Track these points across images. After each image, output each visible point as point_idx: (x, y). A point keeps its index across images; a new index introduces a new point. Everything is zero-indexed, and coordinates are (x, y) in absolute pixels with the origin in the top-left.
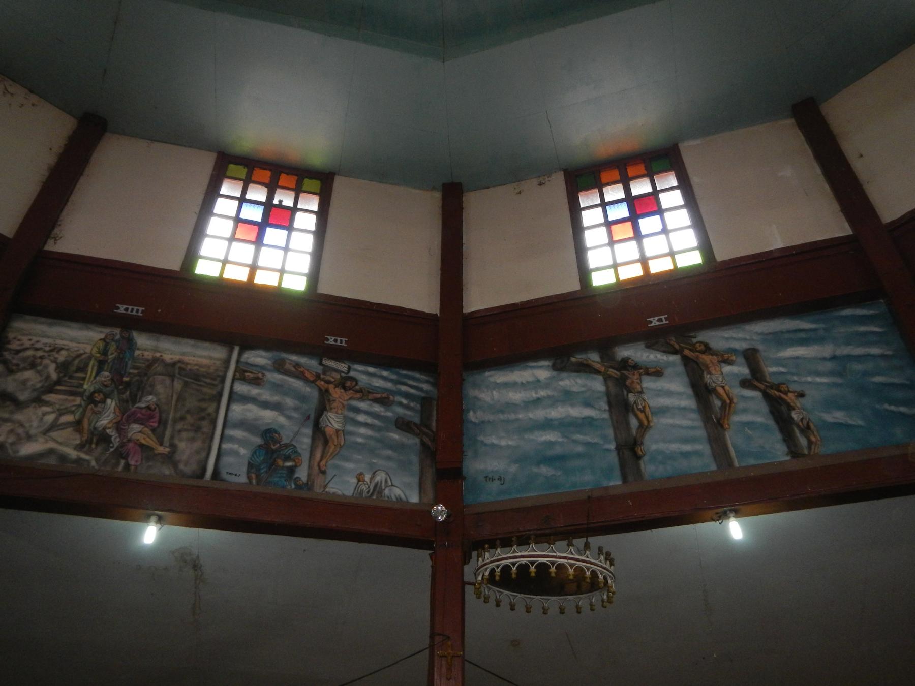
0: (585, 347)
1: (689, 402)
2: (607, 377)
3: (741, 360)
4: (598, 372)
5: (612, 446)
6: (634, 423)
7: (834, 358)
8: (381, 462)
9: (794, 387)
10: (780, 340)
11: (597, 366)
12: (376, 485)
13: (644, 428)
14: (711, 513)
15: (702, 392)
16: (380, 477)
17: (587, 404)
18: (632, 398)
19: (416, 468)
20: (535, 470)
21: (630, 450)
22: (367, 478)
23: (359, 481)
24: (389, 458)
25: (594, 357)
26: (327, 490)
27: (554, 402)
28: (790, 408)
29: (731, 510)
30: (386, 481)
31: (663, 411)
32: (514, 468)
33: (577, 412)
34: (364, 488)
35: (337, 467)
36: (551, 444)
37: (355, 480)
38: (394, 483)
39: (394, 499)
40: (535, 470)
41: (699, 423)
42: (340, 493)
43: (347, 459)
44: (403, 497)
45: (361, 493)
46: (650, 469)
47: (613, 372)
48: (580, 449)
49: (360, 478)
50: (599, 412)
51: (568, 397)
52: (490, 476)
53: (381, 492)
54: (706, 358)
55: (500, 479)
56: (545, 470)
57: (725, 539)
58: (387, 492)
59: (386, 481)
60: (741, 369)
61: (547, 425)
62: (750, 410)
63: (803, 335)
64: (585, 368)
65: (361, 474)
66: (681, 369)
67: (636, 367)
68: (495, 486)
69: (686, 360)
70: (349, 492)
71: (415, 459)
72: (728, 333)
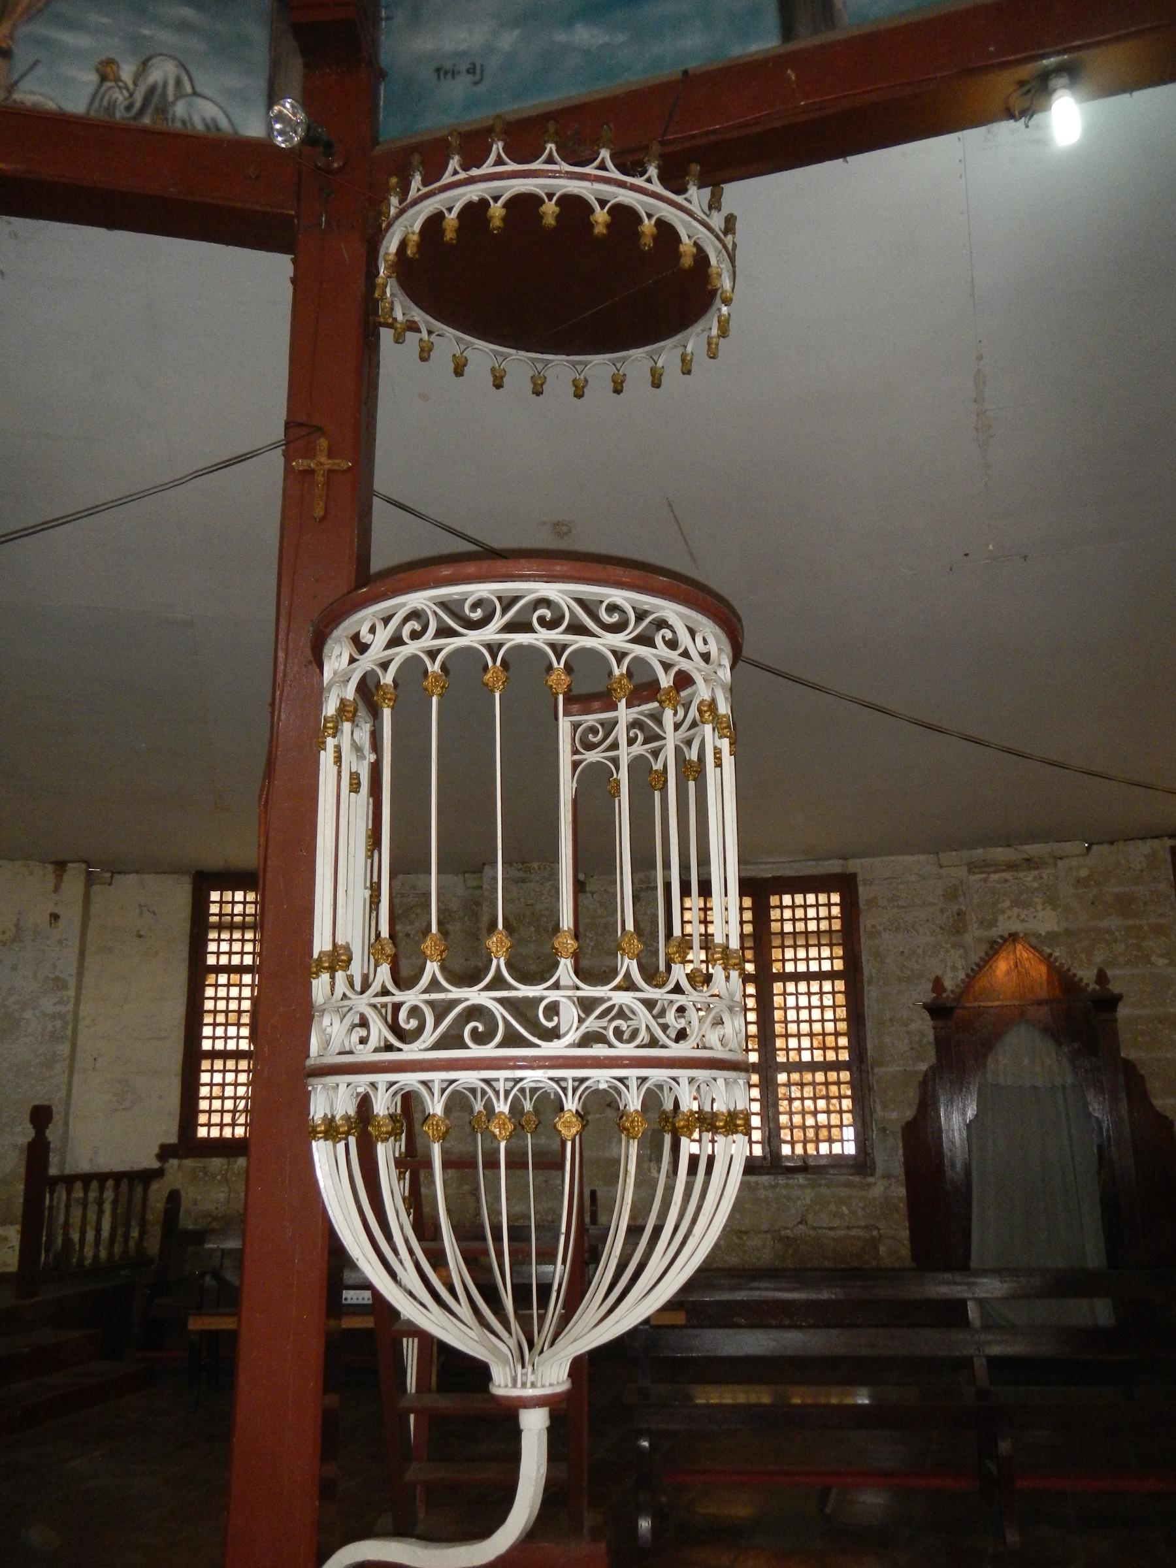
8: (166, 37)
12: (152, 90)
14: (1004, 81)
16: (162, 72)
19: (260, 56)
20: (561, 37)
22: (127, 72)
23: (104, 78)
24: (185, 27)
26: (17, 96)
29: (1060, 69)
30: (178, 82)
32: (508, 40)
34: (120, 97)
35: (41, 42)
37: (93, 78)
38: (199, 89)
39: (200, 126)
40: (561, 37)
42: (51, 105)
43: (71, 25)
44: (224, 123)
45: (112, 105)
49: (106, 72)
52: (448, 65)
53: (163, 110)
55: (471, 71)
58: (180, 109)
59: (178, 82)
65: (110, 62)
68: (458, 89)
70: (76, 104)
71: (258, 34)
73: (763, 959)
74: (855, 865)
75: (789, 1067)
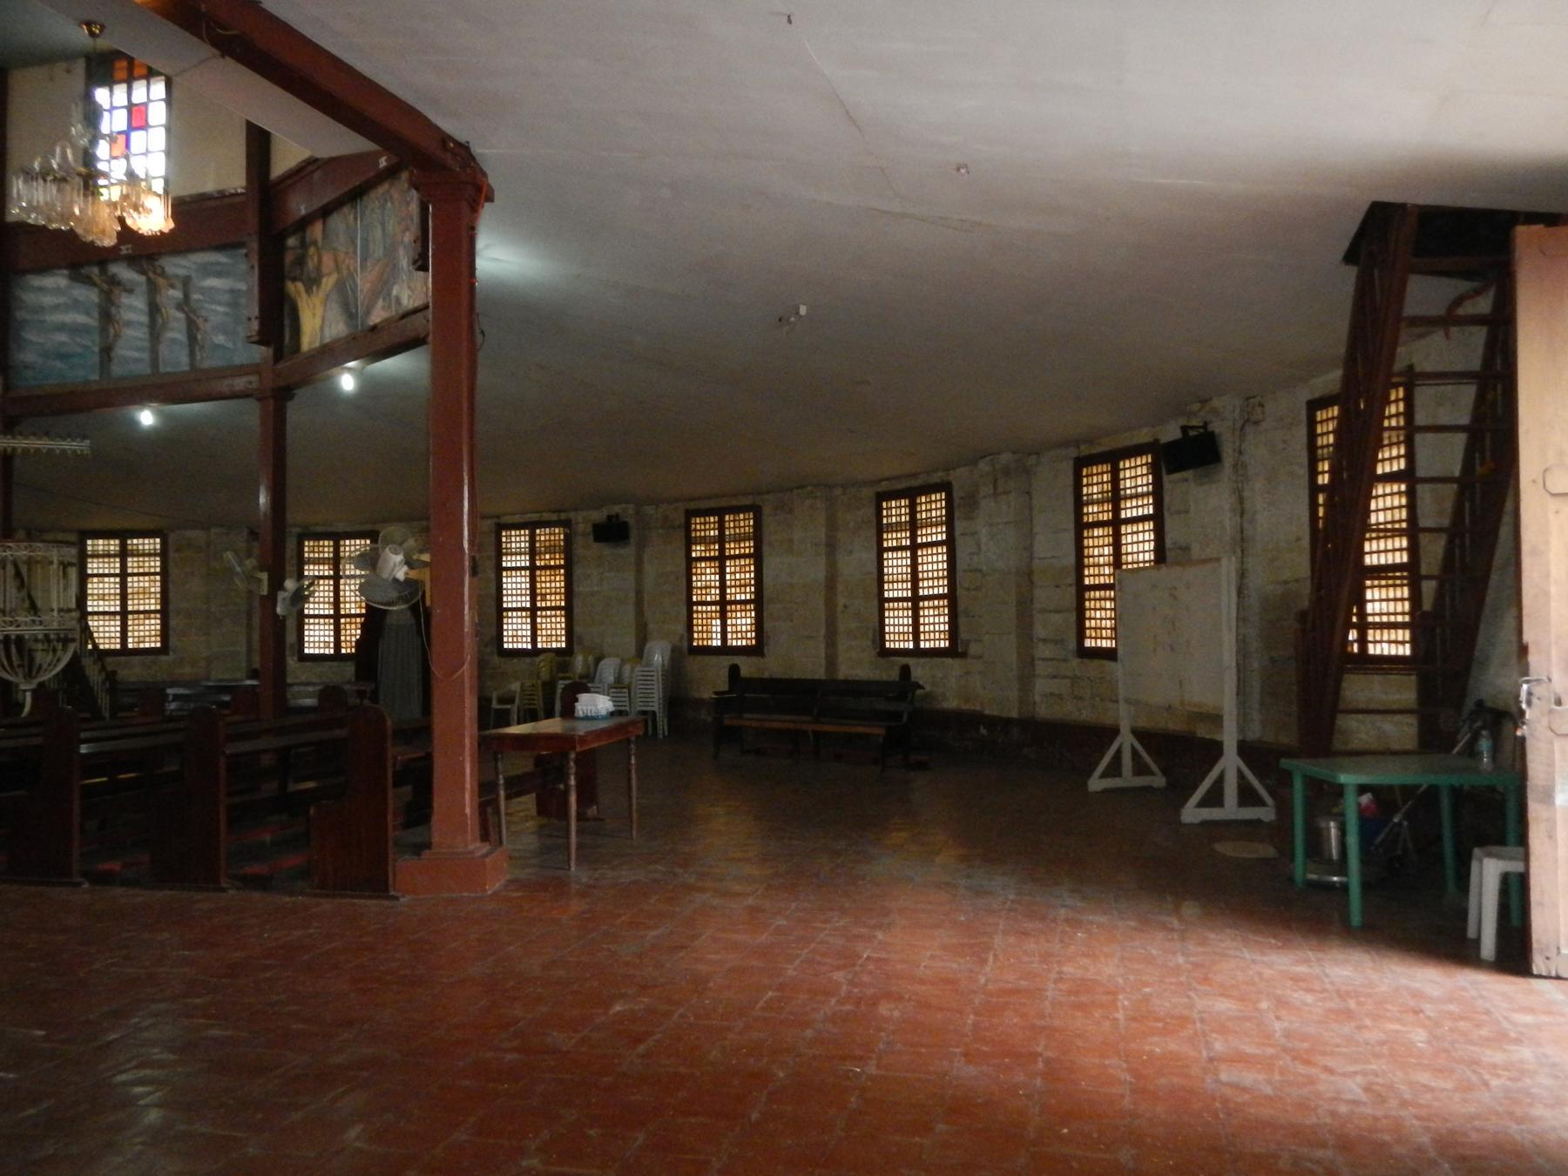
0: (89, 263)
1: (144, 319)
2: (102, 291)
3: (179, 285)
4: (94, 284)
5: (96, 349)
6: (112, 331)
7: (232, 291)
9: (204, 313)
10: (207, 271)
11: (97, 279)
13: (117, 336)
15: (154, 309)
17: (87, 313)
18: (113, 310)
21: (106, 351)
25: (95, 270)
27: (67, 308)
28: (198, 329)
31: (129, 324)
33: (81, 319)
36: (64, 343)
41: (147, 336)
46: (117, 370)
47: (105, 286)
48: (79, 350)
50: (91, 321)
51: (76, 305)
54: (161, 281)
56: (58, 364)
57: (135, 424)
60: (176, 294)
61: (61, 328)
62: (176, 332)
63: (219, 268)
64: (88, 281)
66: (144, 288)
67: (119, 283)
68: (29, 373)
69: (149, 279)
72: (178, 260)
73: (336, 568)
74: (377, 527)
75: (346, 616)
